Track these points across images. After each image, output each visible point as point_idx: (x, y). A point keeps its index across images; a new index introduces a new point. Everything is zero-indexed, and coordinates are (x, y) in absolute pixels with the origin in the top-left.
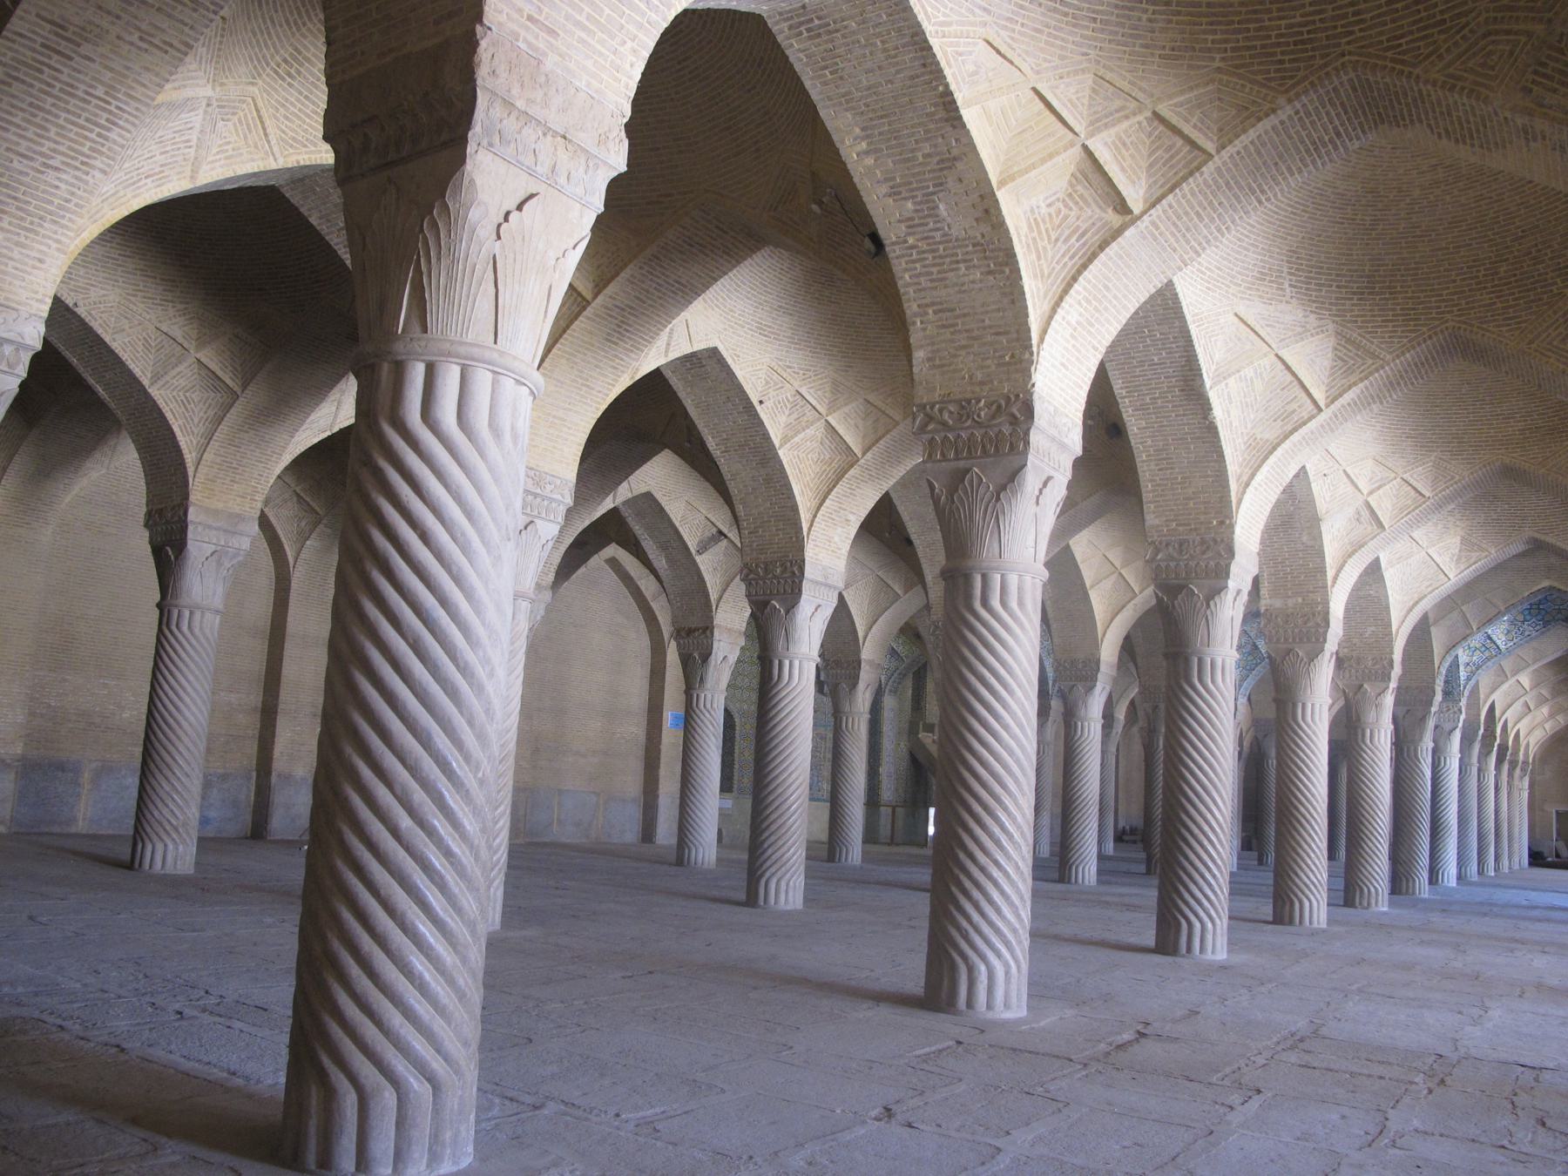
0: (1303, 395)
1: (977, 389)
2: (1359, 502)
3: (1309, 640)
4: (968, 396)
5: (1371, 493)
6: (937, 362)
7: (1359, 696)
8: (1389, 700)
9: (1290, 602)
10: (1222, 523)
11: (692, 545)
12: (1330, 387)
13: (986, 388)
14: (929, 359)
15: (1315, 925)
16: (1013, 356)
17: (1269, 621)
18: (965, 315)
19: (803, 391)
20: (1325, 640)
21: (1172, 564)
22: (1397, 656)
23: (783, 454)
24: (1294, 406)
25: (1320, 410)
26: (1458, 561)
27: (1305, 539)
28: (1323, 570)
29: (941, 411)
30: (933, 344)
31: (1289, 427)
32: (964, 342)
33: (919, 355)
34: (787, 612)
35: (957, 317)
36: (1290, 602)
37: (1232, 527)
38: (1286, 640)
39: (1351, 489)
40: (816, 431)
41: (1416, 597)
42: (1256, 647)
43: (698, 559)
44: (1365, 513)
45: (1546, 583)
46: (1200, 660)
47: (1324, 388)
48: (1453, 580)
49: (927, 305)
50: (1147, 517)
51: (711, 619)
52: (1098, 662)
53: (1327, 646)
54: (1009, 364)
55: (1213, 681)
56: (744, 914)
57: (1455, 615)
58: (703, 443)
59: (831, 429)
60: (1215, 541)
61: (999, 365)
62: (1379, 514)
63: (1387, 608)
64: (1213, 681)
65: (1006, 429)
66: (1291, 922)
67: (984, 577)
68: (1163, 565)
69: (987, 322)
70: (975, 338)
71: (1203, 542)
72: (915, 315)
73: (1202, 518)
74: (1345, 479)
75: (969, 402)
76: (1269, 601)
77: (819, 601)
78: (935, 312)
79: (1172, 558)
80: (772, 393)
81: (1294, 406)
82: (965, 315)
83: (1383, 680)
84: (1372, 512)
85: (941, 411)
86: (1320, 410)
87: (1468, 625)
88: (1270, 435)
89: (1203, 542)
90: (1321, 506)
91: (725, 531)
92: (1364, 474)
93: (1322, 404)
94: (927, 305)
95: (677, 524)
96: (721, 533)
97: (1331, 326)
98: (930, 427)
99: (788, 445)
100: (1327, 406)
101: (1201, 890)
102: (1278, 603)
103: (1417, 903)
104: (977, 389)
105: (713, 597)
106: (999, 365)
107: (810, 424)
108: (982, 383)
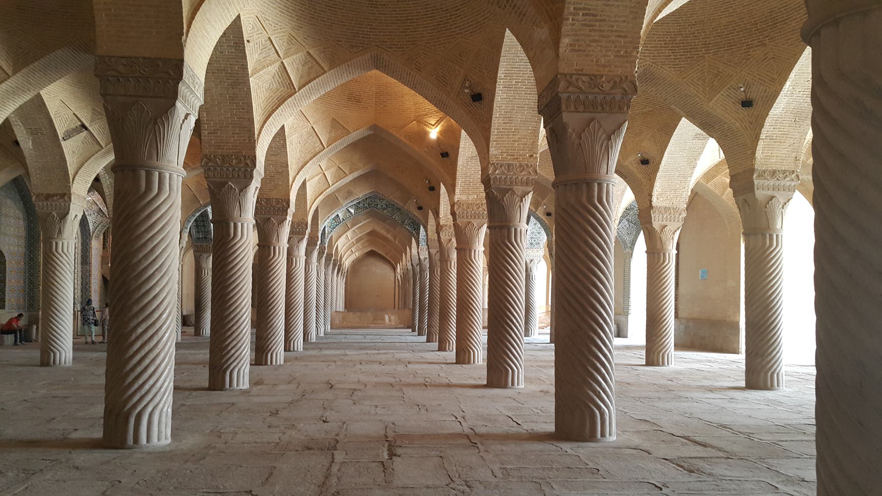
1: (601, 69)
4: (596, 73)
6: (577, 48)
11: (60, 133)
13: (607, 69)
14: (571, 45)
16: (626, 52)
18: (602, 20)
21: (504, 177)
29: (577, 80)
30: (576, 35)
32: (596, 38)
33: (565, 41)
34: (241, 191)
35: (596, 21)
40: (274, 69)
43: (63, 143)
46: (515, 230)
49: (580, 9)
50: (491, 149)
51: (69, 188)
54: (622, 56)
56: (217, 396)
60: (527, 165)
61: (616, 56)
65: (618, 97)
66: (469, 363)
67: (599, 184)
68: (498, 177)
69: (615, 28)
70: (603, 36)
71: (521, 166)
72: (570, 14)
73: (521, 152)
75: (596, 76)
78: (583, 15)
79: (504, 174)
80: (256, 37)
82: (602, 20)
85: (577, 80)
89: (521, 166)
91: (87, 125)
94: (580, 9)
95: (52, 117)
96: (83, 126)
98: (571, 89)
102: (464, 198)
104: (601, 69)
105: (71, 172)
106: (616, 56)
108: (604, 66)
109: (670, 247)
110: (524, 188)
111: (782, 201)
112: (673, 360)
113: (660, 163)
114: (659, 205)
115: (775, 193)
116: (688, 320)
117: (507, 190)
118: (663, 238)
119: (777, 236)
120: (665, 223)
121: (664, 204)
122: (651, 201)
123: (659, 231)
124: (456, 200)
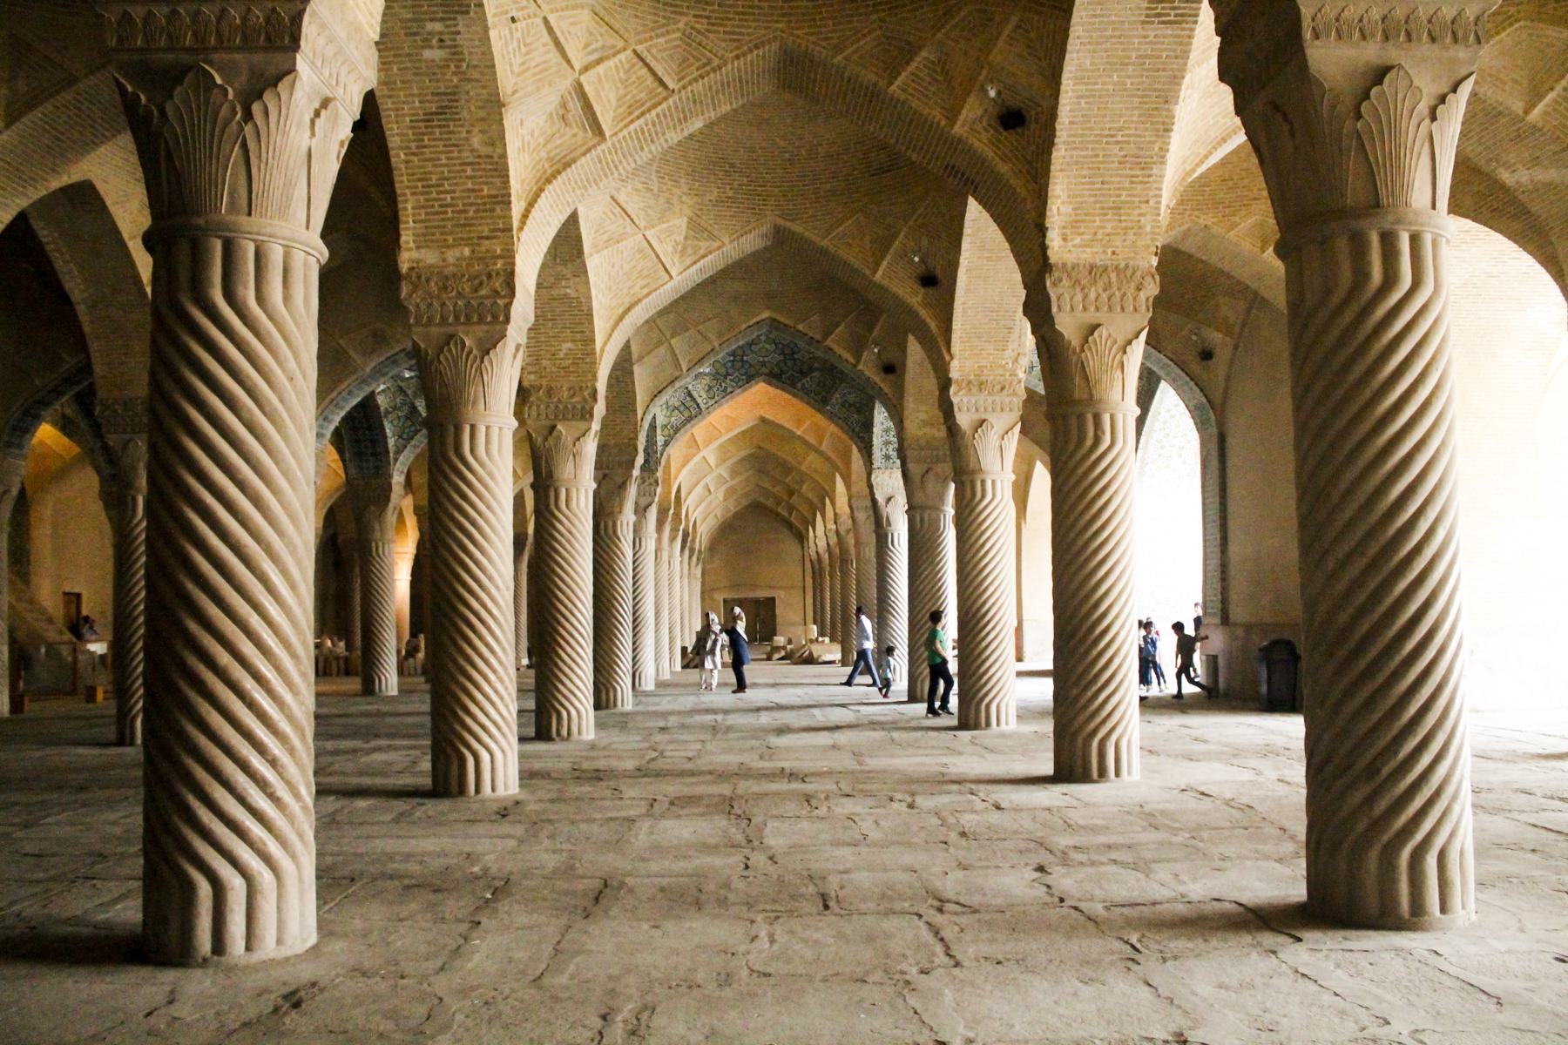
2: (566, 84)
3: (481, 320)
5: (586, 69)
7: (551, 441)
8: (590, 447)
9: (452, 256)
15: (501, 792)
17: (416, 287)
20: (507, 320)
22: (601, 386)
26: (683, 253)
27: (476, 141)
28: (503, 199)
36: (452, 256)
38: (444, 319)
39: (554, 56)
41: (627, 301)
42: (414, 409)
44: (575, 106)
45: (766, 315)
48: (677, 279)
53: (511, 330)
55: (260, 299)
57: (662, 351)
63: (590, 315)
64: (260, 299)
74: (546, 38)
76: (415, 255)
83: (583, 418)
84: (588, 107)
87: (678, 366)
90: (506, 79)
101: (242, 800)
102: (430, 257)
103: (624, 722)
109: (1115, 395)
110: (258, 58)
111: (1428, 88)
112: (1134, 762)
113: (1053, 115)
114: (1069, 258)
115: (1393, 54)
116: (1248, 628)
117: (177, 74)
118: (1092, 364)
119: (1415, 240)
120: (1091, 316)
121: (1086, 256)
122: (1044, 248)
123: (1075, 342)
124: (404, 267)
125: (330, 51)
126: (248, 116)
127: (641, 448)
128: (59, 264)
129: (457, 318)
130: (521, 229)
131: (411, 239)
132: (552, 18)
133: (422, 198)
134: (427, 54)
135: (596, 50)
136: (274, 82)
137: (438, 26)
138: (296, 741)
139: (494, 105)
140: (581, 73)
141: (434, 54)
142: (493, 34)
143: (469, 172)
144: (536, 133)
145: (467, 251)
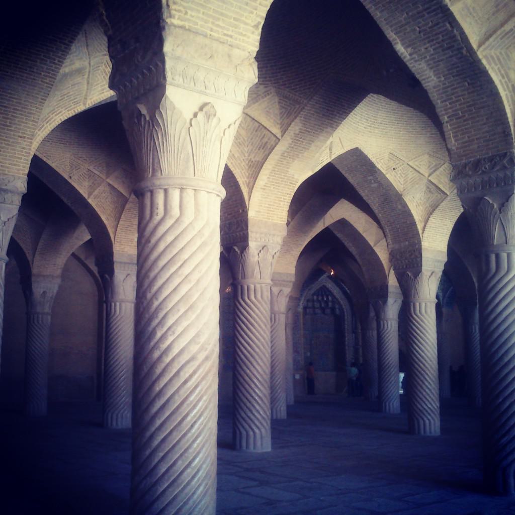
0: (268, 132)
10: (243, 211)
12: (282, 124)
19: (91, 168)
23: (90, 201)
24: (265, 140)
25: (279, 140)
27: (400, 207)
31: (267, 152)
36: (402, 245)
37: (247, 212)
46: (242, 287)
47: (279, 126)
52: (387, 286)
55: (249, 298)
58: (62, 201)
59: (109, 185)
62: (441, 186)
64: (249, 298)
77: (129, 272)
81: (265, 140)
86: (279, 140)
88: (259, 158)
92: (423, 163)
93: (279, 136)
97: (273, 90)
99: (92, 196)
100: (282, 136)
107: (99, 185)
125: (263, 235)
126: (242, 257)
127: (103, 364)
128: (346, 244)
129: (406, 267)
130: (423, 233)
131: (390, 241)
132: (410, 163)
133: (390, 227)
134: (373, 186)
135: (433, 167)
136: (245, 249)
137: (371, 178)
138: (436, 413)
139: (399, 197)
140: (429, 176)
141: (376, 185)
142: (387, 176)
143: (401, 217)
144: (422, 199)
145: (407, 243)
